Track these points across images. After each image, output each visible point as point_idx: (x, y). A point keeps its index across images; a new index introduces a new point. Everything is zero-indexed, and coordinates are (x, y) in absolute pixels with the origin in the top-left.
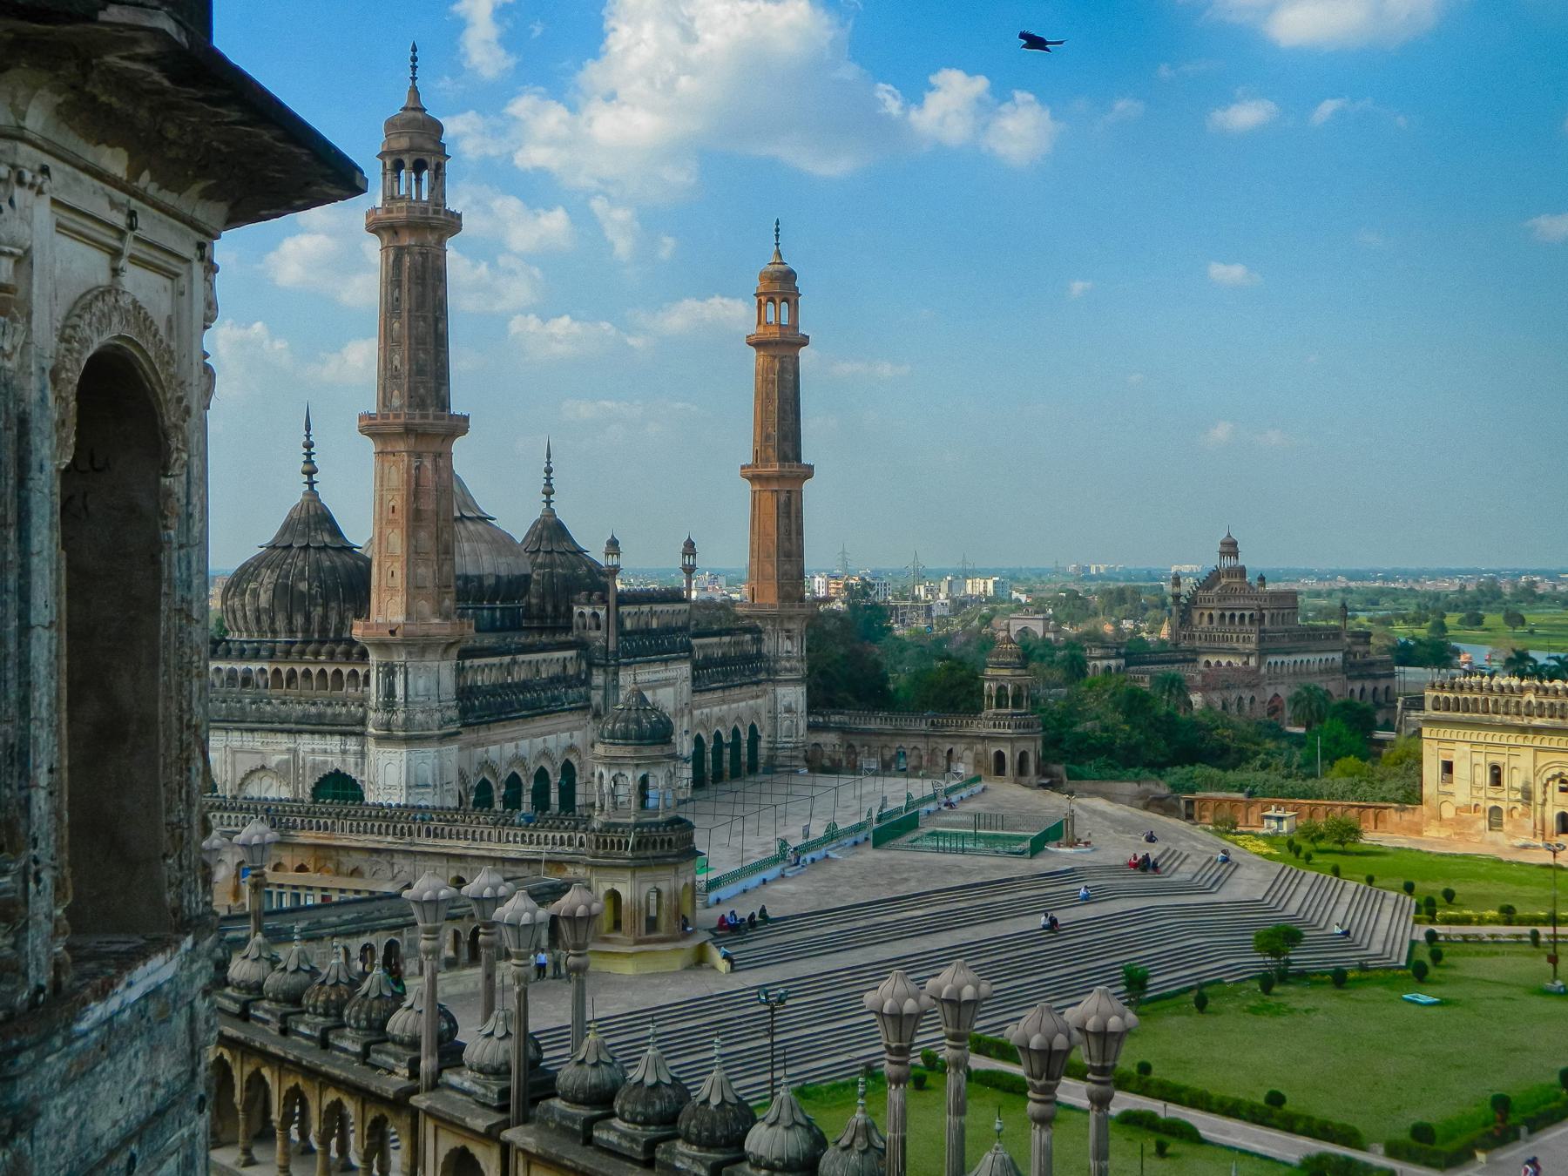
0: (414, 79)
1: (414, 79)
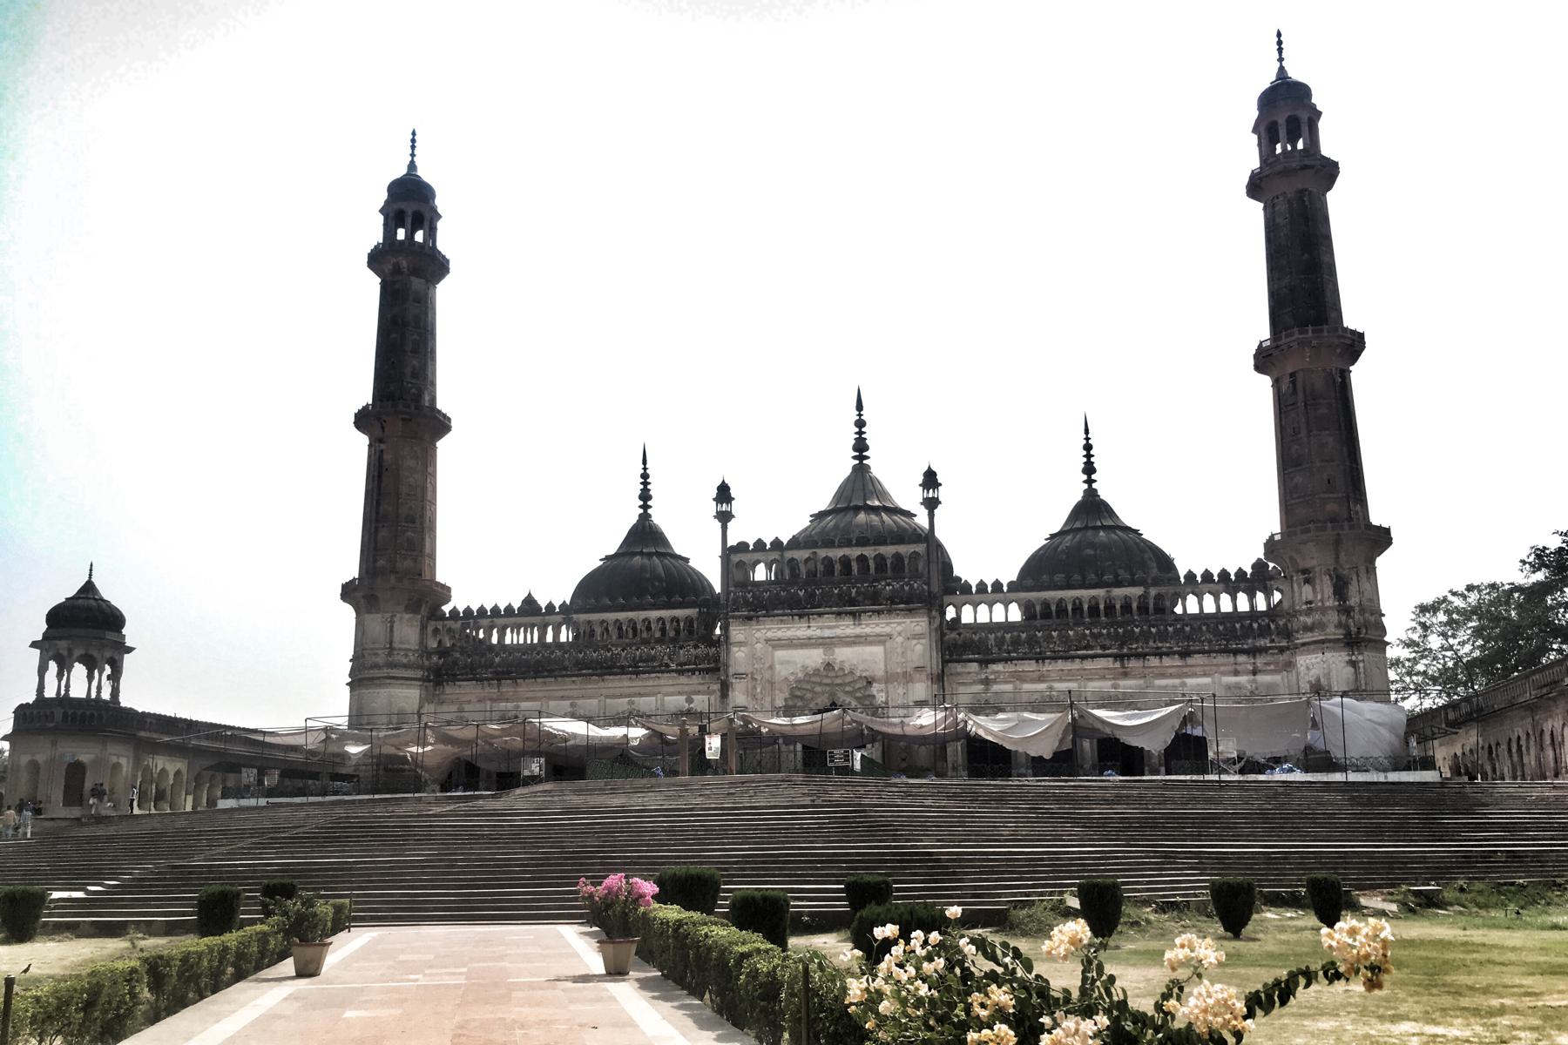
0: (413, 155)
1: (413, 155)
